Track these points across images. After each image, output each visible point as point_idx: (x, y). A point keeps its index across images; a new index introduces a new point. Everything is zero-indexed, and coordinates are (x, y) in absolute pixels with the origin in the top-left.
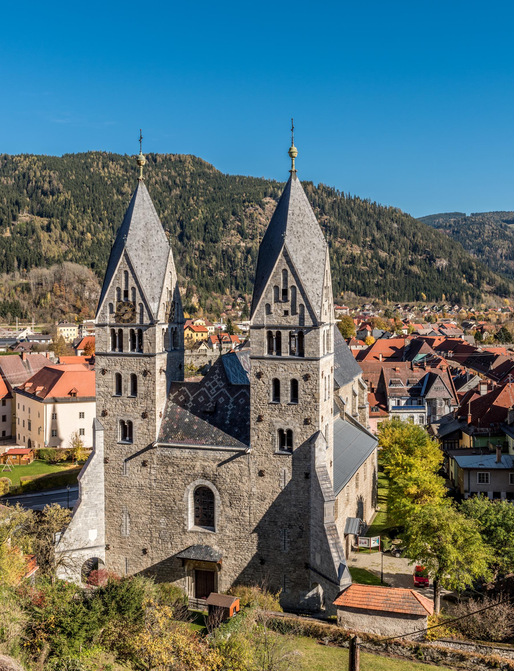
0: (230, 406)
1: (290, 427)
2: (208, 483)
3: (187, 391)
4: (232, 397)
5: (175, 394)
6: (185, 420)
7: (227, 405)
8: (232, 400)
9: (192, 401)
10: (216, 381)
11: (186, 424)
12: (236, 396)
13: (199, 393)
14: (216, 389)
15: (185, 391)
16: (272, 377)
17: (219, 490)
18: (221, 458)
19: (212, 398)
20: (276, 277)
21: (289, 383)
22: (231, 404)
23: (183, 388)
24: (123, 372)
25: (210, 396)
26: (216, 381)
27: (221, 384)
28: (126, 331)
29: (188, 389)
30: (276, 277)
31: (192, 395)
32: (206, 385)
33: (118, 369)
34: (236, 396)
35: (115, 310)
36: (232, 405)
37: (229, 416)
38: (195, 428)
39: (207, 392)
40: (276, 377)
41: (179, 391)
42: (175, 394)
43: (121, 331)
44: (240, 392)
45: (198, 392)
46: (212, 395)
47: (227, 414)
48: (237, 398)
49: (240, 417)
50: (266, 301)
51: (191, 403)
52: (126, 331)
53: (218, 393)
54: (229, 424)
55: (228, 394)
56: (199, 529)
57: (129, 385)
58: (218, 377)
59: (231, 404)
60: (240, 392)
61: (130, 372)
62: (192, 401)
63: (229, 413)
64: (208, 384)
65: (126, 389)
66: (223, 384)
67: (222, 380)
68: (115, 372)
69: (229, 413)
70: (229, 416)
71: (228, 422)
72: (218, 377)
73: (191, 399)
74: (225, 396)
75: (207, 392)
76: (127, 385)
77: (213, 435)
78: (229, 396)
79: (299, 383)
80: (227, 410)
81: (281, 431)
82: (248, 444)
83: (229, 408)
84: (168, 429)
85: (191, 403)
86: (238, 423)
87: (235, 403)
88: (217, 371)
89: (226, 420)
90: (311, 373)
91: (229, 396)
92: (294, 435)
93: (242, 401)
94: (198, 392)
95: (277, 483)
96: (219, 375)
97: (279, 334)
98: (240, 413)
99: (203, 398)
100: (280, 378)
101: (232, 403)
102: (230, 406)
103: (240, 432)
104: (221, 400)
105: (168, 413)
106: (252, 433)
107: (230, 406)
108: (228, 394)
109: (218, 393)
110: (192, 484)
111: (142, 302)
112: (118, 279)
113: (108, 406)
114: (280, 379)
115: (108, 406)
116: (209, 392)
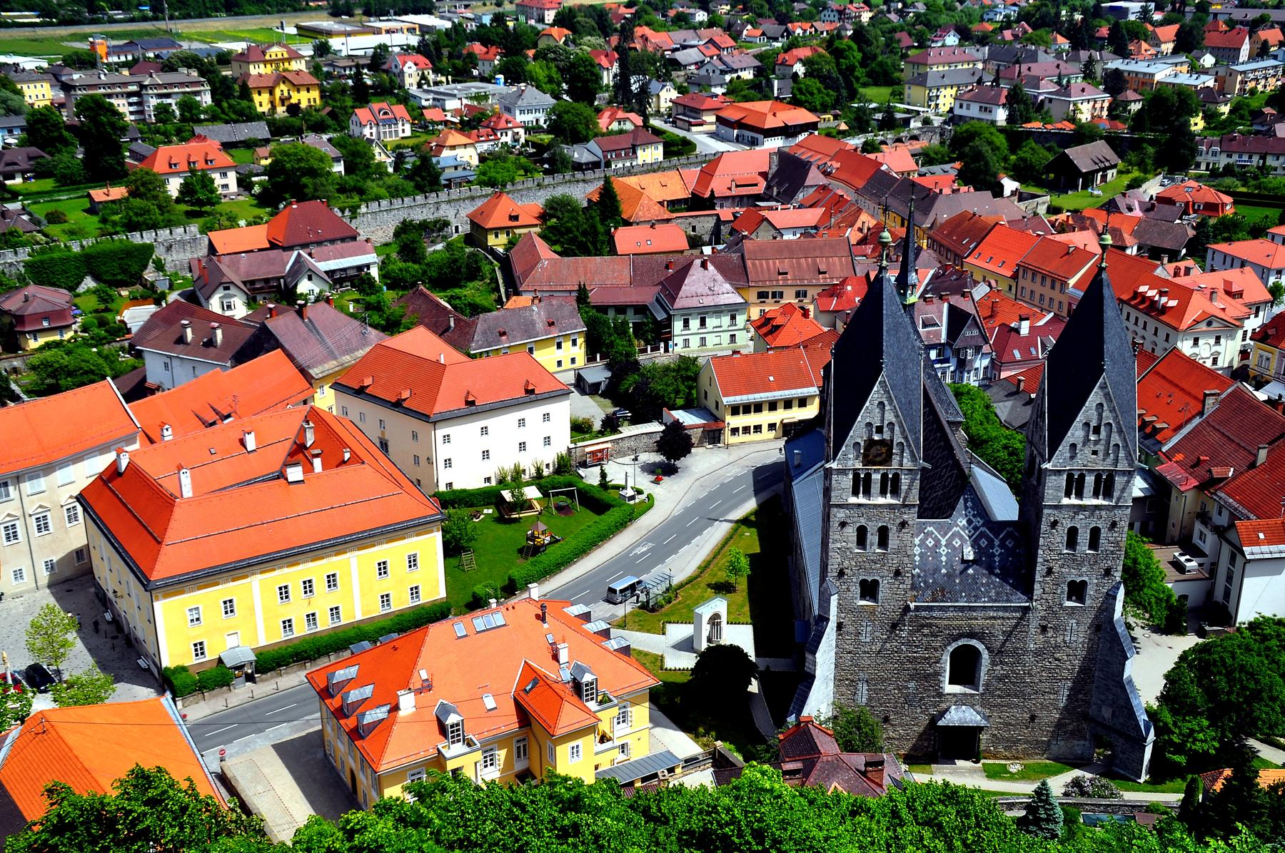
1: (1086, 579)
2: (974, 642)
8: (997, 542)
17: (988, 648)
28: (876, 477)
31: (943, 537)
33: (863, 522)
43: (868, 476)
50: (1072, 441)
52: (876, 477)
56: (957, 689)
57: (876, 539)
63: (997, 559)
65: (872, 544)
73: (943, 542)
74: (987, 538)
76: (873, 538)
82: (1030, 599)
87: (1002, 545)
90: (1117, 519)
97: (1082, 477)
104: (984, 543)
106: (1037, 586)
107: (997, 551)
112: (869, 411)
113: (846, 563)
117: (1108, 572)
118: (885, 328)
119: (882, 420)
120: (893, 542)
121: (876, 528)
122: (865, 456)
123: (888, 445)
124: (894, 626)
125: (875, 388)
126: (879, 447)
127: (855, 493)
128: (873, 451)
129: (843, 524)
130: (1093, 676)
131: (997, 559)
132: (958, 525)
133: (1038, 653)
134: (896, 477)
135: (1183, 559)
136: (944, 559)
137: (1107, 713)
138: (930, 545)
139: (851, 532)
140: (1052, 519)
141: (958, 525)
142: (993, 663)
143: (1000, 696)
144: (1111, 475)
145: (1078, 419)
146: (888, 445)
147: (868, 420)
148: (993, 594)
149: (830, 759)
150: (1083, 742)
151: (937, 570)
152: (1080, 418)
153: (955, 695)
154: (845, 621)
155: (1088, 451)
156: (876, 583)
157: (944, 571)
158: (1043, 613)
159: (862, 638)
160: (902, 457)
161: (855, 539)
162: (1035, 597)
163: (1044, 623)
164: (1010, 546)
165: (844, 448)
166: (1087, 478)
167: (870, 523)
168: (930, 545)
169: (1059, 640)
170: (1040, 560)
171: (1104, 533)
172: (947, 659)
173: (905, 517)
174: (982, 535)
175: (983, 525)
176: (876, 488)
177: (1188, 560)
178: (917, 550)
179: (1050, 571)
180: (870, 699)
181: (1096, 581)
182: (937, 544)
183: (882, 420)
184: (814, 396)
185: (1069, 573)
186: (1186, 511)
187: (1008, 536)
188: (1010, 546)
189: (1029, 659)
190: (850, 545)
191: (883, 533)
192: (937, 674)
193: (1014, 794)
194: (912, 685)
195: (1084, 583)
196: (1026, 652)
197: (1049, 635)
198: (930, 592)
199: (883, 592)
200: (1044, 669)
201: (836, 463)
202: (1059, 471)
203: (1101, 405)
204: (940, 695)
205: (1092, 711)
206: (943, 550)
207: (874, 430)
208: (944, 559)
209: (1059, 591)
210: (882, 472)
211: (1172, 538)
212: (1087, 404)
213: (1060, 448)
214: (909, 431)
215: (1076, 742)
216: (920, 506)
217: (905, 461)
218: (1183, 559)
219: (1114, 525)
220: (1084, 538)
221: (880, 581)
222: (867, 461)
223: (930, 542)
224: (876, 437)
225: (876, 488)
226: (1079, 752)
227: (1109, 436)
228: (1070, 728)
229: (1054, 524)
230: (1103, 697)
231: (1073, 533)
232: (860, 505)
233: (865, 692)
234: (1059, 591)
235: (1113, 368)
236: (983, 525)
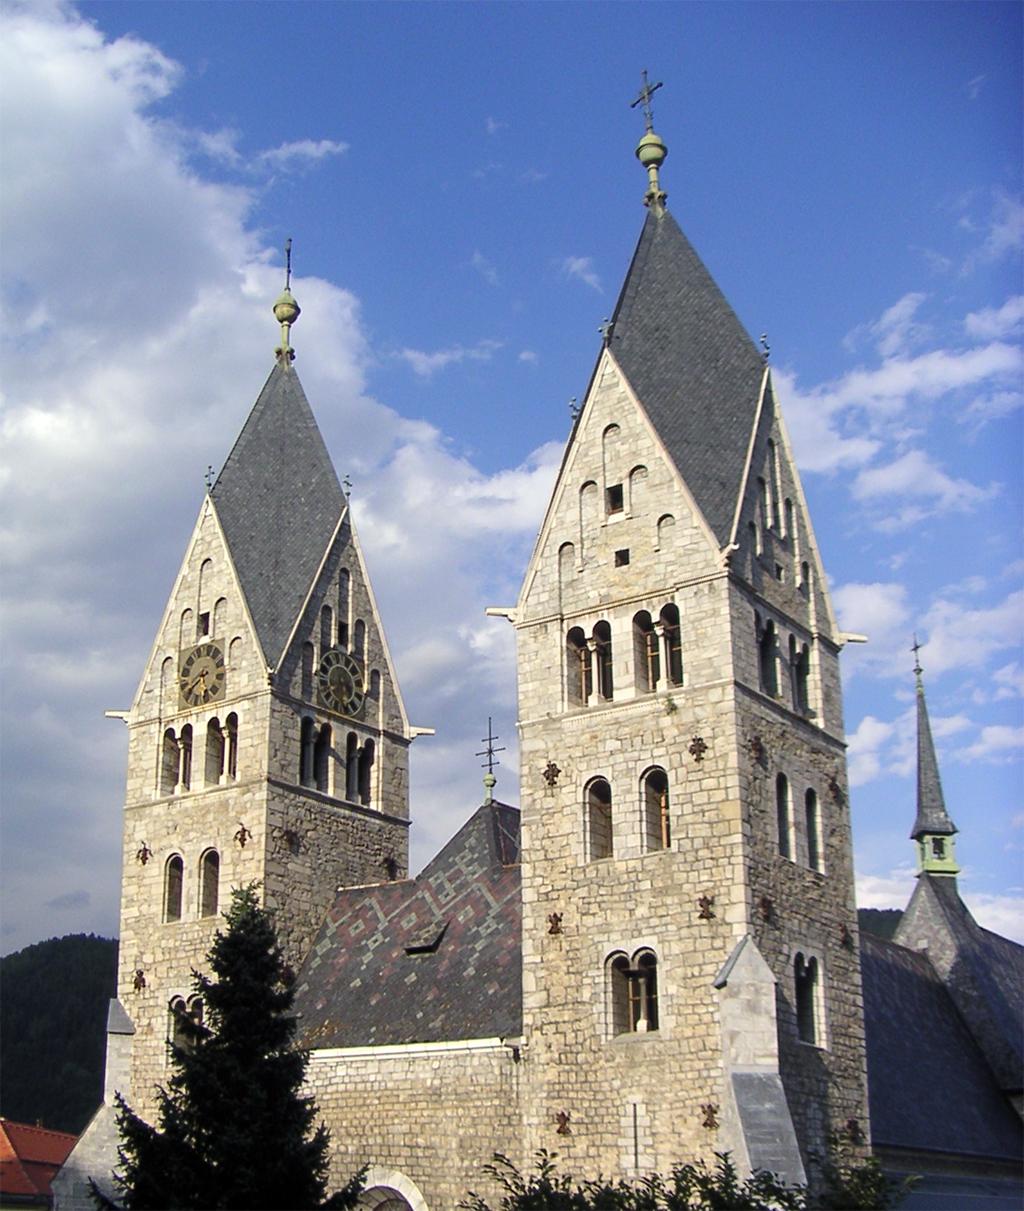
0: (488, 927)
1: (650, 941)
3: (377, 907)
4: (497, 901)
9: (385, 934)
10: (463, 868)
14: (455, 889)
15: (372, 908)
18: (437, 1082)
19: (439, 914)
24: (187, 849)
25: (435, 910)
28: (200, 731)
29: (379, 902)
30: (586, 455)
33: (174, 845)
39: (429, 899)
40: (599, 773)
43: (187, 730)
46: (441, 907)
47: (473, 950)
51: (379, 936)
54: (473, 977)
59: (489, 920)
63: (479, 946)
65: (190, 902)
67: (480, 861)
69: (479, 946)
70: (477, 954)
71: (471, 971)
75: (429, 899)
77: (420, 1015)
78: (490, 898)
80: (476, 937)
81: (620, 964)
85: (379, 936)
86: (500, 970)
88: (472, 841)
90: (705, 734)
92: (661, 971)
96: (472, 850)
97: (603, 629)
100: (608, 775)
102: (488, 927)
106: (529, 982)
113: (148, 958)
114: (609, 779)
115: (148, 958)
116: (436, 900)
117: (706, 908)
129: (144, 855)
140: (543, 765)
144: (671, 613)
158: (552, 1074)
162: (527, 1019)
163: (559, 1107)
167: (187, 847)
168: (353, 933)
179: (555, 924)
181: (676, 948)
185: (605, 929)
208: (368, 958)
209: (586, 995)
210: (209, 716)
219: (698, 748)
234: (586, 995)
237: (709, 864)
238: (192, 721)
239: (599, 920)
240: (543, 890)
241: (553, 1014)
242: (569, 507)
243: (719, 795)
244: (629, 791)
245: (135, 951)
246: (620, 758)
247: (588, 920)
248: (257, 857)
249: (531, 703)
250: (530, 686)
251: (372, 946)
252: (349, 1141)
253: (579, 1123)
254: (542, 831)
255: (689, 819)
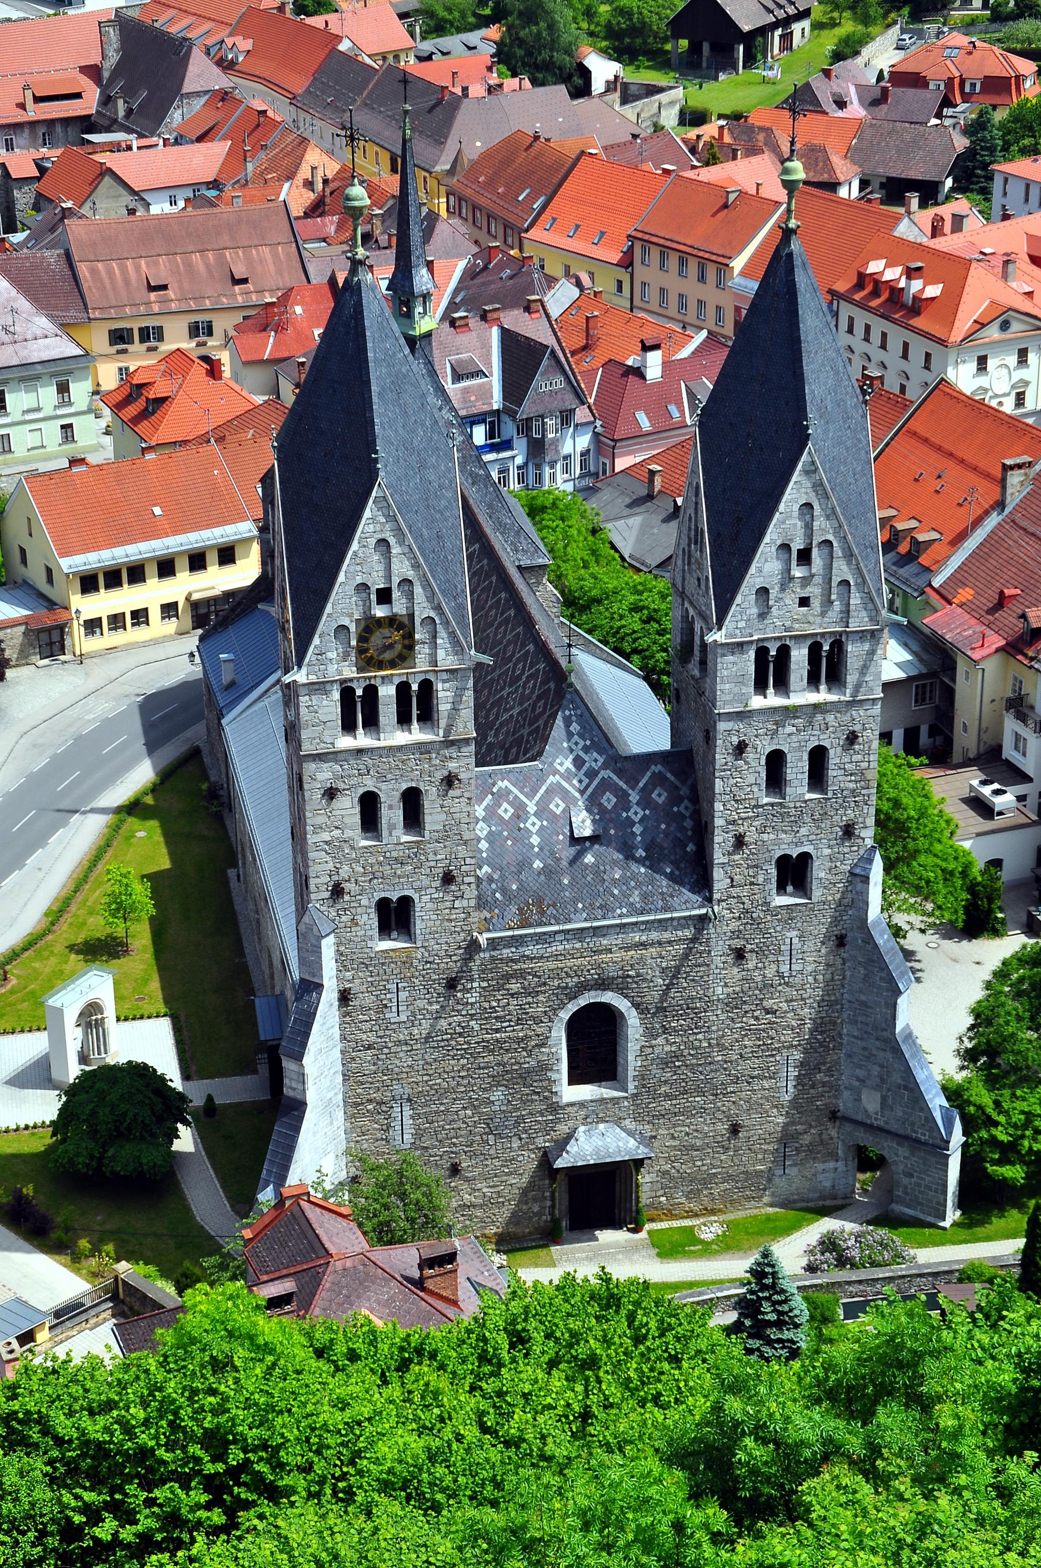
0: (636, 813)
1: (808, 848)
2: (609, 997)
5: (485, 804)
6: (535, 866)
7: (628, 810)
8: (634, 797)
9: (536, 814)
11: (539, 873)
12: (641, 785)
13: (546, 791)
14: (586, 774)
15: (509, 792)
16: (768, 750)
17: (636, 1006)
20: (784, 523)
21: (806, 757)
22: (635, 808)
23: (500, 783)
26: (581, 753)
27: (596, 760)
28: (387, 692)
30: (784, 523)
32: (559, 767)
33: (369, 784)
34: (641, 785)
35: (354, 643)
36: (639, 810)
37: (639, 838)
38: (566, 882)
41: (493, 794)
42: (485, 804)
43: (371, 691)
44: (649, 774)
45: (544, 788)
47: (633, 833)
48: (645, 792)
49: (666, 835)
50: (759, 583)
51: (533, 819)
52: (387, 692)
53: (595, 783)
55: (621, 783)
56: (586, 1092)
58: (582, 743)
60: (649, 774)
61: (404, 786)
62: (536, 814)
63: (637, 829)
64: (561, 764)
65: (392, 827)
66: (601, 760)
68: (361, 791)
70: (639, 838)
72: (582, 743)
73: (532, 808)
76: (392, 814)
78: (625, 786)
79: (832, 752)
83: (633, 817)
84: (498, 895)
87: (645, 802)
89: (636, 848)
90: (857, 728)
91: (625, 786)
93: (659, 795)
94: (544, 788)
95: (774, 967)
97: (784, 651)
98: (663, 826)
99: (560, 802)
101: (638, 804)
103: (677, 873)
104: (609, 800)
105: (484, 855)
106: (718, 874)
107: (636, 813)
108: (621, 783)
109: (595, 783)
110: (569, 1006)
111: (432, 614)
113: (345, 871)
117: (848, 831)
118: (374, 388)
119: (389, 577)
120: (433, 817)
121: (397, 795)
122: (361, 651)
123: (403, 626)
124: (452, 984)
125: (367, 514)
126: (386, 632)
127: (348, 726)
128: (376, 639)
129: (331, 794)
130: (840, 1035)
131: (637, 829)
132: (556, 772)
133: (733, 1003)
134: (427, 686)
135: (987, 791)
136: (535, 840)
137: (871, 1103)
138: (506, 817)
139: (348, 808)
140: (735, 740)
141: (556, 772)
142: (650, 1034)
143: (668, 1096)
144: (838, 645)
145: (767, 539)
146: (403, 626)
147: (359, 580)
148: (636, 898)
149: (349, 1263)
150: (832, 1165)
151: (524, 864)
152: (772, 536)
153: (582, 1104)
154: (355, 987)
155: (791, 600)
156: (406, 903)
157: (538, 864)
158: (734, 925)
159: (392, 1016)
160: (434, 646)
161: (357, 819)
162: (716, 896)
163: (738, 943)
164: (660, 801)
165: (316, 641)
166: (794, 653)
167: (384, 786)
168: (506, 817)
169: (770, 972)
170: (719, 822)
171: (835, 757)
172: (559, 1035)
173: (452, 765)
174: (605, 785)
175: (605, 766)
176: (388, 711)
177: (997, 792)
178: (482, 830)
179: (740, 842)
180: (418, 1135)
181: (827, 851)
182: (520, 812)
183: (389, 577)
184: (247, 541)
186: (987, 699)
187: (658, 780)
188: (660, 801)
189: (717, 1017)
190: (348, 834)
191: (412, 800)
192: (544, 1068)
193: (714, 1282)
194: (497, 1095)
195: (805, 857)
196: (710, 1003)
197: (751, 965)
198: (514, 909)
199: (423, 919)
200: (748, 1030)
201: (304, 670)
202: (741, 645)
203: (808, 506)
204: (555, 1108)
205: (844, 1104)
206: (533, 824)
207: (374, 597)
208: (535, 840)
209: (761, 879)
210: (397, 681)
211: (965, 751)
212: (782, 507)
213: (739, 599)
214: (443, 592)
215: (820, 1166)
216: (479, 742)
217: (441, 654)
218: (987, 791)
219: (852, 738)
220: (797, 770)
221: (416, 897)
222: (367, 661)
223: (506, 811)
224: (380, 612)
225: (388, 711)
226: (828, 1184)
227: (829, 567)
228: (806, 1139)
229: (740, 749)
230: (860, 1073)
231: (776, 762)
232: (360, 751)
233: (408, 1122)
235: (826, 432)
236: (605, 766)
237: (853, 804)
238: (377, 682)
239: (772, 836)
240: (731, 818)
241: (734, 891)
242: (766, 561)
243: (865, 765)
244: (801, 760)
245: (331, 866)
246: (794, 738)
247: (765, 836)
248: (467, 795)
249: (728, 697)
250: (727, 686)
251: (534, 830)
252: (569, 980)
253: (752, 951)
254: (732, 781)
255: (841, 778)
